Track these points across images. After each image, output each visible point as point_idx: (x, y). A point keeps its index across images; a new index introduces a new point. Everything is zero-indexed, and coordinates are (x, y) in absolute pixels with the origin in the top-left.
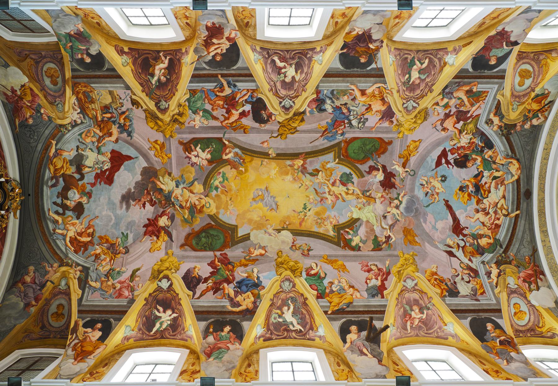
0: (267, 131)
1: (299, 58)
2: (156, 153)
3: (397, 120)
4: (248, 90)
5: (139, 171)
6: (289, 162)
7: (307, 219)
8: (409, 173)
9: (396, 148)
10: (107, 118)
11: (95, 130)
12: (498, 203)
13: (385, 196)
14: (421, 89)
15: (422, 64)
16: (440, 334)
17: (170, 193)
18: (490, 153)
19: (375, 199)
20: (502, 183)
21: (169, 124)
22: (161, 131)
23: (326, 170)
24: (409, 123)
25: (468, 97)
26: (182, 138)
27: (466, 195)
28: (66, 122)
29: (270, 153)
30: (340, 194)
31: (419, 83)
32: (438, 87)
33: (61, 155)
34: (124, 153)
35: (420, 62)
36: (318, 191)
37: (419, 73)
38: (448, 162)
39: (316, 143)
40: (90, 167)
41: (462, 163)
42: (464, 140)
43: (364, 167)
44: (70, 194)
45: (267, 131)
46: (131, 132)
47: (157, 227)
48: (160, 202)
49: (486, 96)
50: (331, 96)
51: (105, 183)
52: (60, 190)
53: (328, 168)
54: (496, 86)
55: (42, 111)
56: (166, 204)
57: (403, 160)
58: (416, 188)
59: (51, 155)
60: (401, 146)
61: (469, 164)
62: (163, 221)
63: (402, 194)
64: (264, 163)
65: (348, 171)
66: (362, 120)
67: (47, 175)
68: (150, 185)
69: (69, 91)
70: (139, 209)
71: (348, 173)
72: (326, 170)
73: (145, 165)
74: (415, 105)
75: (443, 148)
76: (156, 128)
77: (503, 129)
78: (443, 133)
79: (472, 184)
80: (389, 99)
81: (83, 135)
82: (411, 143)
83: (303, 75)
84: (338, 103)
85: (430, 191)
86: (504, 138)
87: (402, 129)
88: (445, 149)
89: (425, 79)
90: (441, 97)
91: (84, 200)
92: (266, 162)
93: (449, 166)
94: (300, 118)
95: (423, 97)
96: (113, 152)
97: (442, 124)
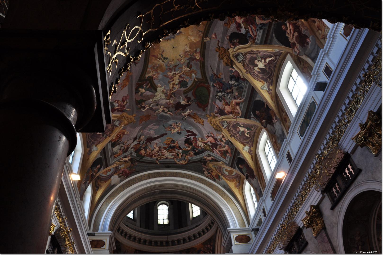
0: (223, 39)
1: (269, 72)
3: (217, 116)
4: (255, 36)
6: (199, 50)
7: (157, 60)
8: (183, 118)
9: (200, 113)
12: (164, 156)
13: (171, 105)
14: (234, 131)
15: (247, 133)
16: (90, 143)
18: (192, 154)
19: (169, 99)
20: (174, 158)
23: (191, 73)
24: (215, 122)
25: (224, 150)
27: (169, 143)
29: (208, 38)
30: (173, 80)
31: (237, 130)
32: (233, 140)
35: (248, 133)
36: (177, 67)
37: (243, 131)
38: (188, 136)
39: (210, 69)
41: (187, 141)
42: (200, 144)
43: (190, 95)
45: (223, 39)
49: (223, 158)
50: (240, 86)
53: (192, 74)
54: (228, 163)
57: (192, 115)
58: (175, 120)
60: (201, 115)
61: (186, 145)
63: (171, 113)
64: (200, 33)
65: (189, 85)
66: (220, 99)
71: (187, 85)
72: (191, 73)
74: (225, 126)
75: (197, 134)
77: (204, 160)
78: (206, 136)
79: (175, 145)
80: (231, 116)
82: (203, 121)
83: (257, 73)
84: (234, 88)
85: (172, 127)
86: (199, 160)
87: (212, 117)
88: (197, 135)
89: (238, 134)
90: (227, 139)
92: (201, 35)
93: (187, 136)
94: (229, 64)
95: (228, 131)
97: (211, 136)
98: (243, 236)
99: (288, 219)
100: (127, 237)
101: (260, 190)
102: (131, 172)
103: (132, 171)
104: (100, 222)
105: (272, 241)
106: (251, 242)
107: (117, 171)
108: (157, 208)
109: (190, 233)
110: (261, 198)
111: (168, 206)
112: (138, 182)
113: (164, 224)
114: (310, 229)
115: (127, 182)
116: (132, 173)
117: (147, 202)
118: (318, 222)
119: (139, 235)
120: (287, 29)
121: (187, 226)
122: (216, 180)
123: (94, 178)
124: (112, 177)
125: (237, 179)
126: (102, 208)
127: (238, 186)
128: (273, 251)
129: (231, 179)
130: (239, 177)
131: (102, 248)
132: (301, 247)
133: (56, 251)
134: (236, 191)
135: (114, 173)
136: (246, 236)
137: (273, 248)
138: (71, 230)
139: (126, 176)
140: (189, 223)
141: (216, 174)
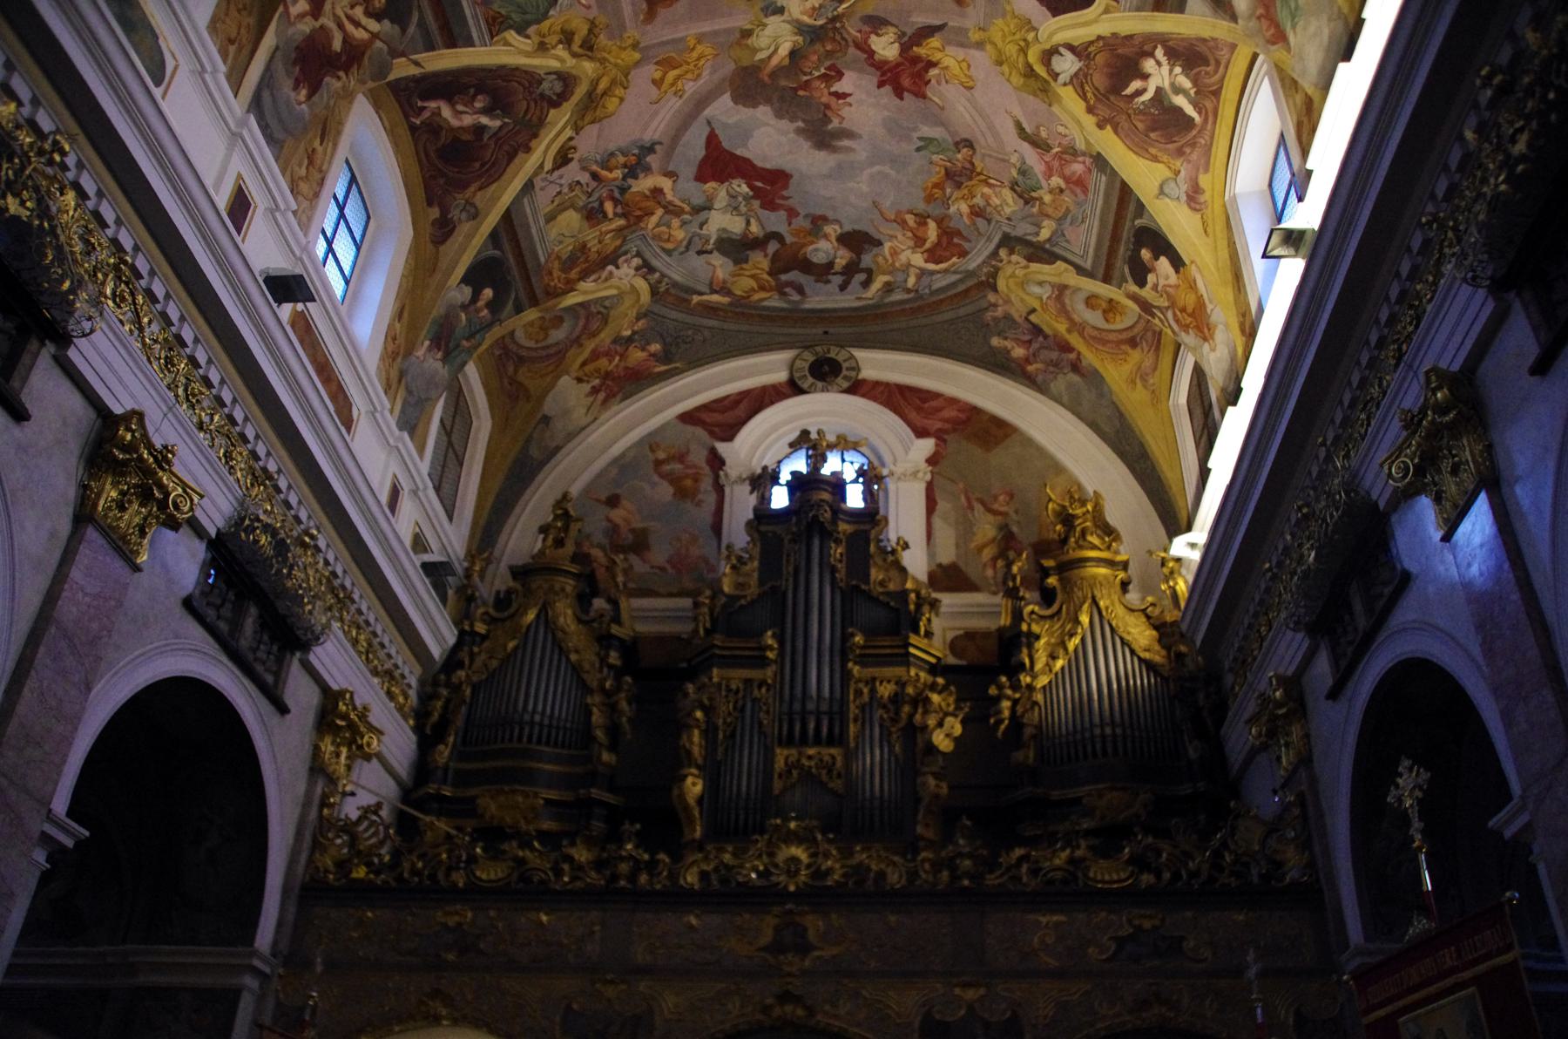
2: (689, 76)
5: (744, 113)
10: (615, 206)
11: (650, 226)
17: (800, 28)
21: (603, 61)
22: (626, 76)
26: (636, 15)
28: (642, 285)
33: (724, 282)
34: (700, 152)
40: (748, 223)
44: (819, 258)
46: (642, 148)
47: (902, 64)
48: (829, 54)
51: (786, 186)
52: (811, 278)
55: (628, 333)
56: (834, 40)
59: (725, 300)
62: (886, 47)
67: (775, 302)
68: (783, 83)
69: (571, 300)
70: (853, 109)
73: (726, 99)
76: (619, 91)
81: (669, 246)
91: (832, 230)
96: (701, 178)
120: (368, 14)
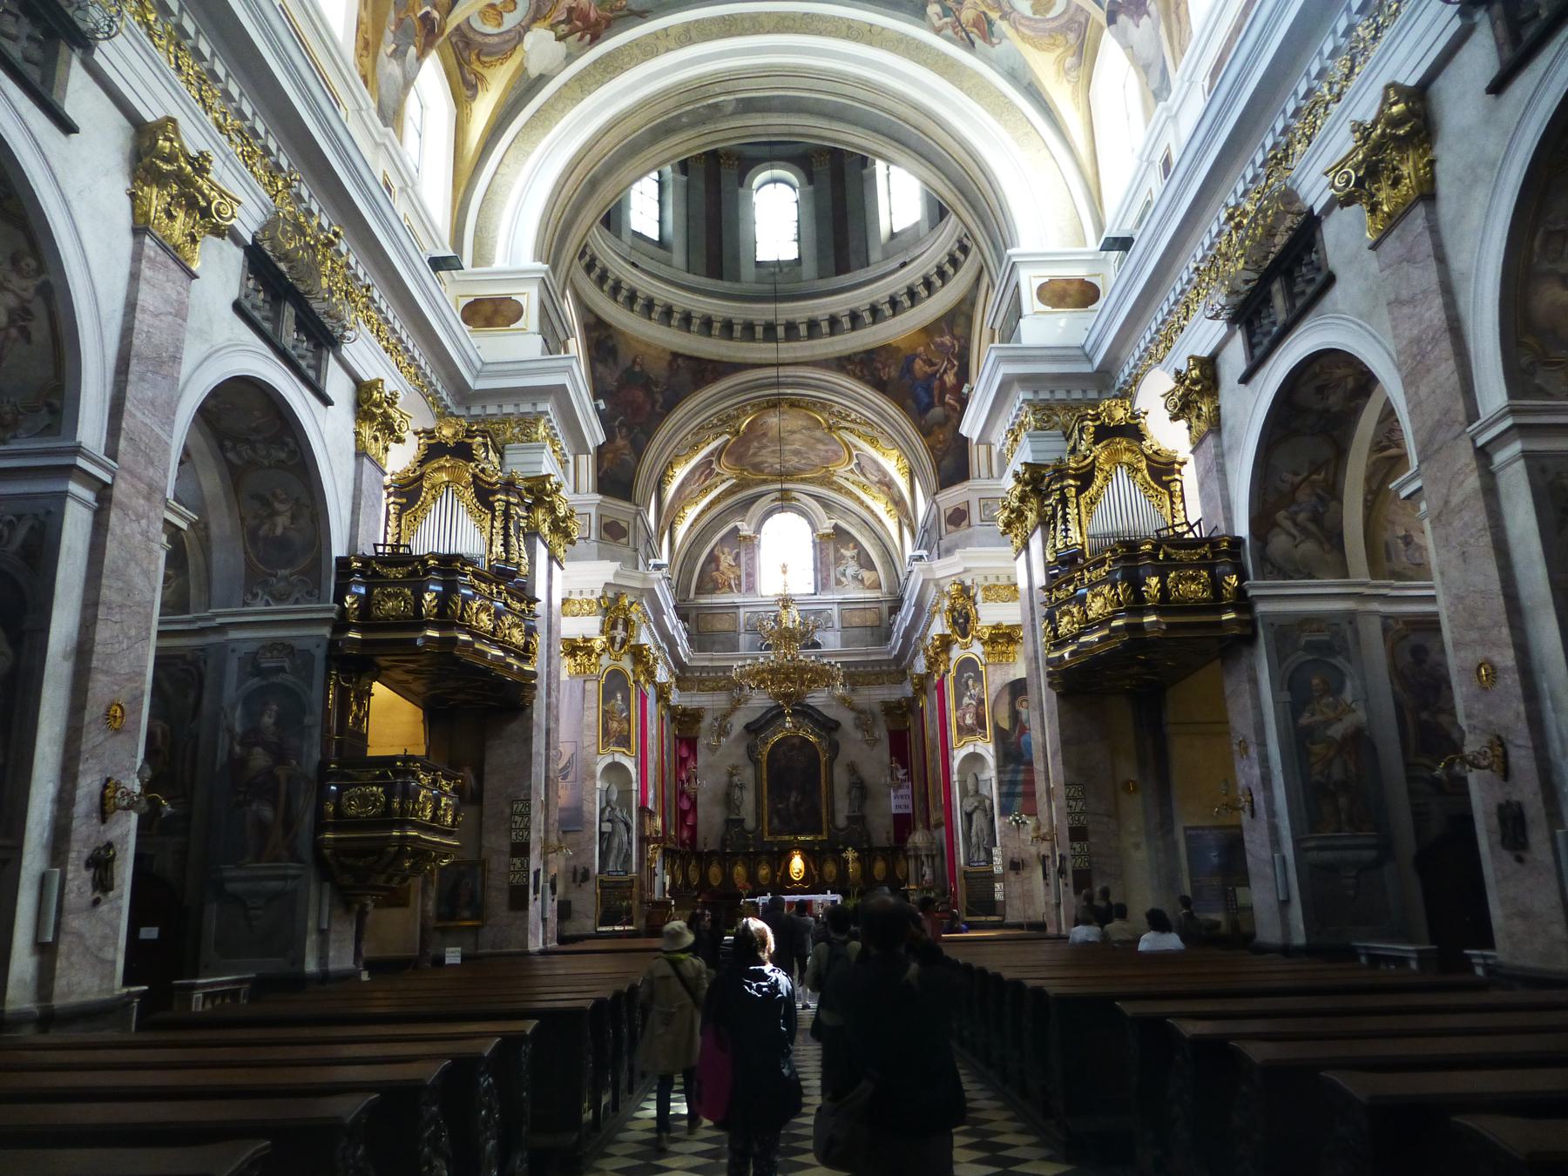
98: (1069, 281)
99: (1263, 184)
100: (637, 308)
101: (1164, 71)
102: (611, 15)
103: (612, 11)
104: (497, 228)
105: (1183, 292)
106: (1098, 305)
107: (546, 11)
108: (751, 197)
109: (878, 292)
110: (1161, 104)
111: (794, 189)
112: (643, 61)
113: (781, 259)
114: (1357, 211)
115: (595, 62)
116: (615, 19)
117: (688, 151)
118: (1406, 169)
119: (682, 300)
121: (868, 265)
122: (979, 42)
123: (442, 31)
124: (529, 39)
125: (1072, 37)
126: (503, 175)
127: (1069, 69)
128: (1182, 330)
129: (1046, 37)
130: (1080, 23)
131: (512, 326)
132: (1299, 303)
133: (286, 313)
134: (1060, 92)
135: (534, 20)
136: (1082, 281)
137: (1185, 319)
138: (336, 234)
139: (588, 37)
140: (875, 255)
141: (978, 16)
